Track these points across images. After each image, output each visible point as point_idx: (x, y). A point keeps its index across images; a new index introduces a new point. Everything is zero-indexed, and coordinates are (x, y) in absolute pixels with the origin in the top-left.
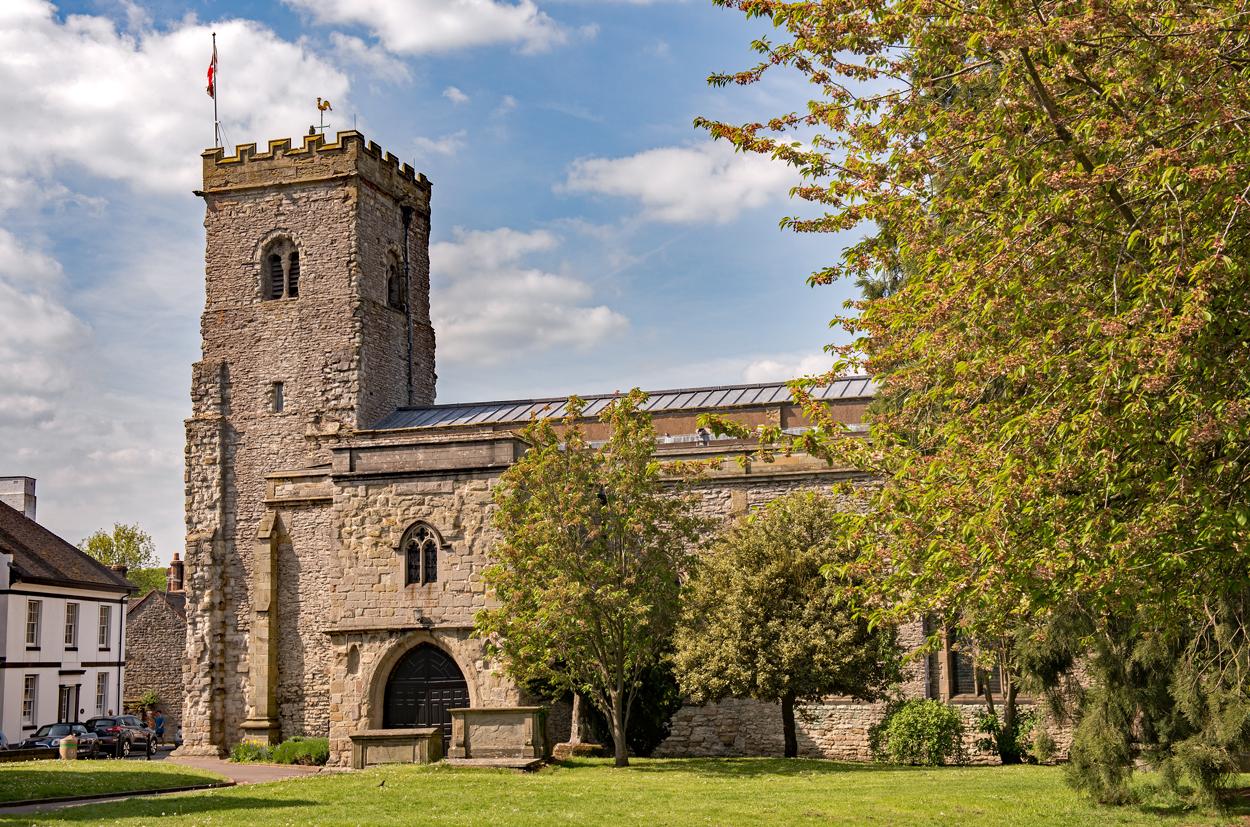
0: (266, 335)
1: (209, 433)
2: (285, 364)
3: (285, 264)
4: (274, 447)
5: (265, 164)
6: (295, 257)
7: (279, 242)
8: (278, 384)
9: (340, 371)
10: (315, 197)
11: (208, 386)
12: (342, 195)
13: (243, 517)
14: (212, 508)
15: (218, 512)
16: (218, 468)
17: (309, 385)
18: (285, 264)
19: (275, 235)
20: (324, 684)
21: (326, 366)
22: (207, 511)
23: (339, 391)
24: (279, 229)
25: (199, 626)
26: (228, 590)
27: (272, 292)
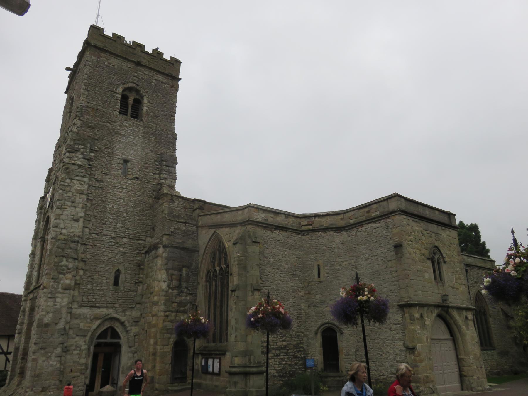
0: (122, 132)
1: (82, 174)
2: (132, 152)
3: (131, 101)
4: (122, 195)
5: (131, 50)
6: (138, 102)
7: (130, 89)
8: (126, 161)
9: (167, 166)
10: (156, 78)
11: (80, 147)
12: (171, 84)
13: (96, 232)
14: (77, 221)
15: (81, 224)
16: (85, 197)
17: (146, 168)
18: (131, 101)
19: (131, 85)
20: (283, 341)
21: (156, 161)
22: (72, 222)
23: (165, 176)
24: (134, 83)
25: (59, 300)
26: (78, 278)
27: (123, 111)
